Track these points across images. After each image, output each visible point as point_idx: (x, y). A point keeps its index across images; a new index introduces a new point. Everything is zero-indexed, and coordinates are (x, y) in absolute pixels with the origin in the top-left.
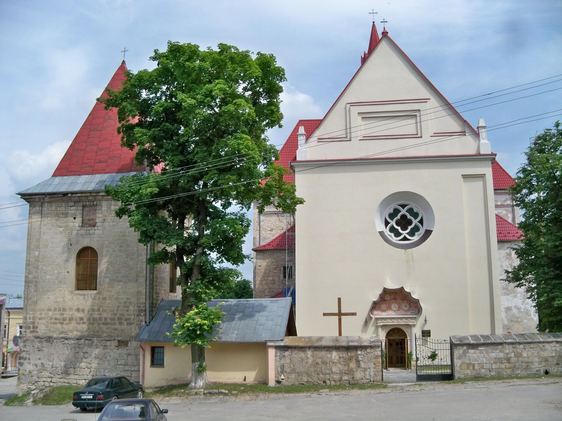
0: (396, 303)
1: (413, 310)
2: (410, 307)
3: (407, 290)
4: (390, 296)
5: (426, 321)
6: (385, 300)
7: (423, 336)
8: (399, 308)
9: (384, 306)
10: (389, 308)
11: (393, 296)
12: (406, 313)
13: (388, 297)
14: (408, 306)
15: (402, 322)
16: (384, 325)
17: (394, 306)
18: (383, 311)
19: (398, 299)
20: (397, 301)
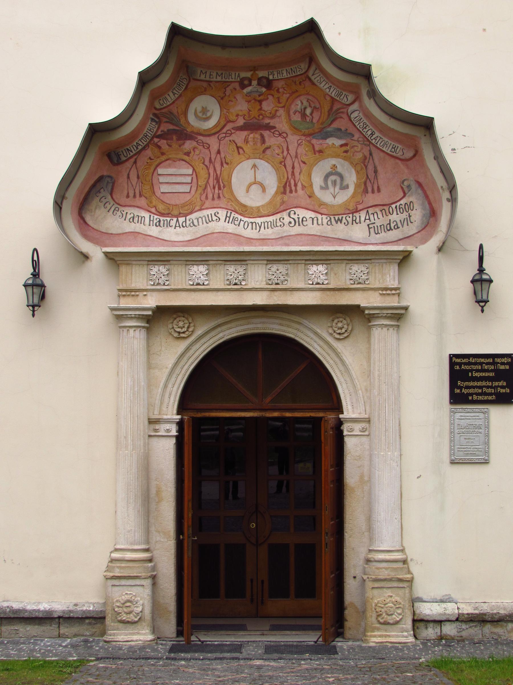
0: (264, 153)
1: (385, 207)
2: (368, 185)
3: (345, 41)
4: (223, 101)
5: (481, 281)
6: (183, 134)
7: (457, 398)
8: (286, 187)
9: (174, 178)
10: (216, 189)
11: (241, 106)
12: (340, 230)
13: (205, 113)
14: (351, 178)
15: (305, 288)
16: (162, 313)
17: (253, 178)
18: (169, 212)
19: (281, 123)
20: (272, 140)
